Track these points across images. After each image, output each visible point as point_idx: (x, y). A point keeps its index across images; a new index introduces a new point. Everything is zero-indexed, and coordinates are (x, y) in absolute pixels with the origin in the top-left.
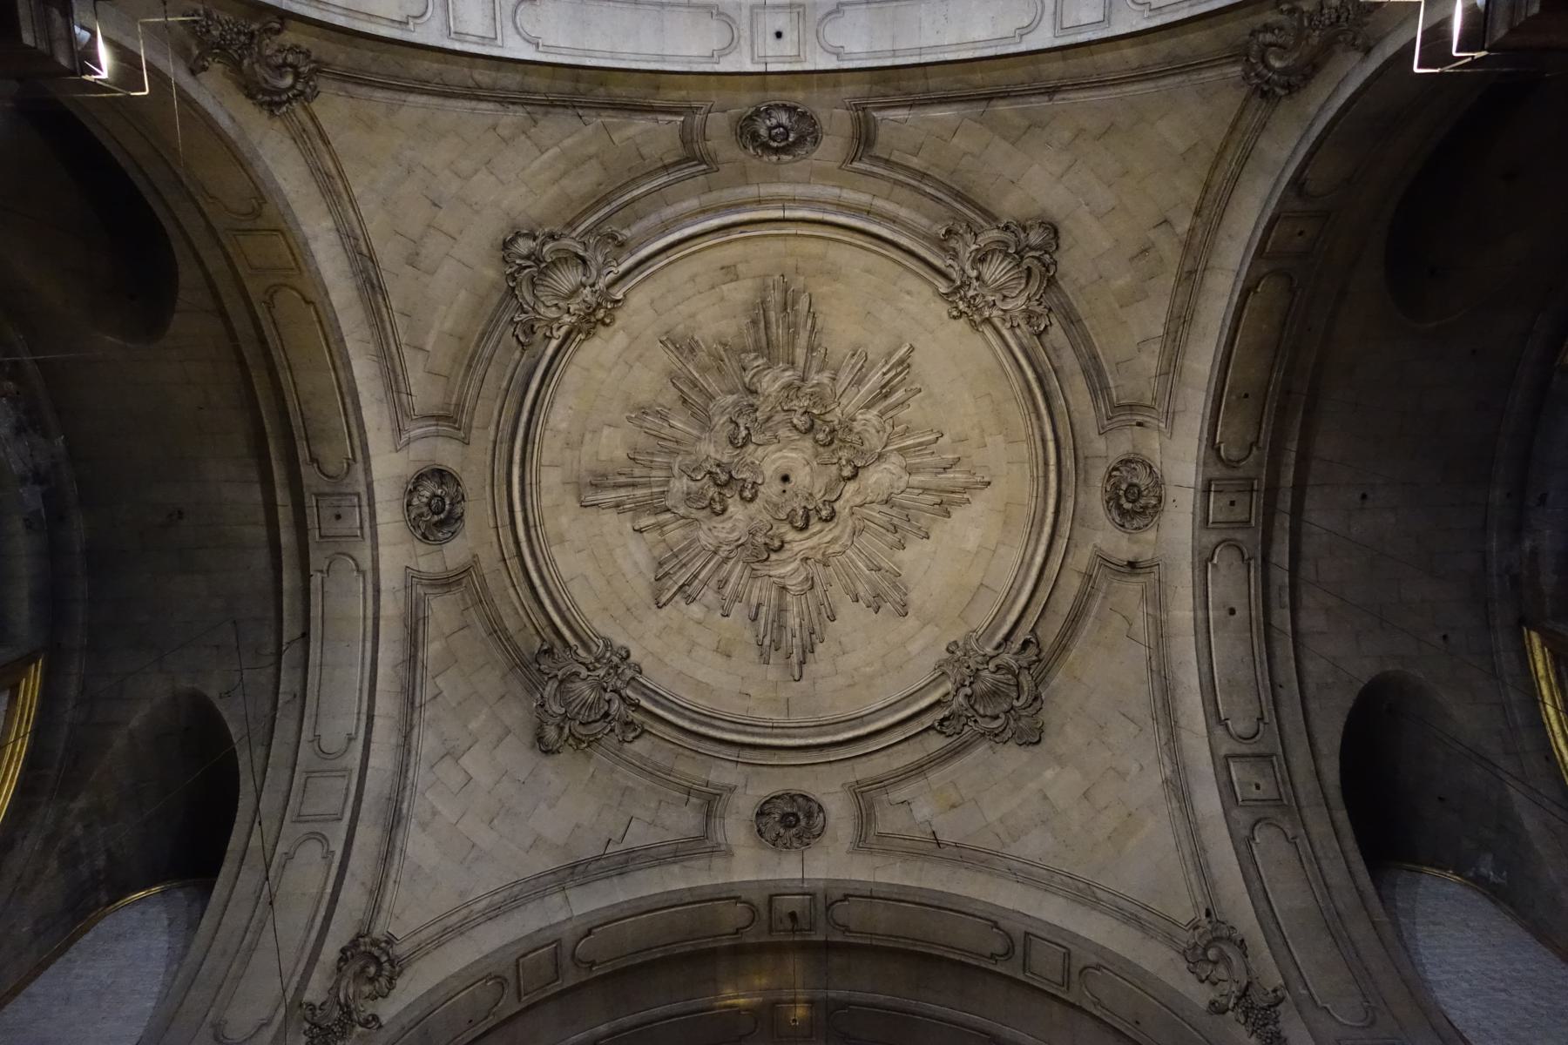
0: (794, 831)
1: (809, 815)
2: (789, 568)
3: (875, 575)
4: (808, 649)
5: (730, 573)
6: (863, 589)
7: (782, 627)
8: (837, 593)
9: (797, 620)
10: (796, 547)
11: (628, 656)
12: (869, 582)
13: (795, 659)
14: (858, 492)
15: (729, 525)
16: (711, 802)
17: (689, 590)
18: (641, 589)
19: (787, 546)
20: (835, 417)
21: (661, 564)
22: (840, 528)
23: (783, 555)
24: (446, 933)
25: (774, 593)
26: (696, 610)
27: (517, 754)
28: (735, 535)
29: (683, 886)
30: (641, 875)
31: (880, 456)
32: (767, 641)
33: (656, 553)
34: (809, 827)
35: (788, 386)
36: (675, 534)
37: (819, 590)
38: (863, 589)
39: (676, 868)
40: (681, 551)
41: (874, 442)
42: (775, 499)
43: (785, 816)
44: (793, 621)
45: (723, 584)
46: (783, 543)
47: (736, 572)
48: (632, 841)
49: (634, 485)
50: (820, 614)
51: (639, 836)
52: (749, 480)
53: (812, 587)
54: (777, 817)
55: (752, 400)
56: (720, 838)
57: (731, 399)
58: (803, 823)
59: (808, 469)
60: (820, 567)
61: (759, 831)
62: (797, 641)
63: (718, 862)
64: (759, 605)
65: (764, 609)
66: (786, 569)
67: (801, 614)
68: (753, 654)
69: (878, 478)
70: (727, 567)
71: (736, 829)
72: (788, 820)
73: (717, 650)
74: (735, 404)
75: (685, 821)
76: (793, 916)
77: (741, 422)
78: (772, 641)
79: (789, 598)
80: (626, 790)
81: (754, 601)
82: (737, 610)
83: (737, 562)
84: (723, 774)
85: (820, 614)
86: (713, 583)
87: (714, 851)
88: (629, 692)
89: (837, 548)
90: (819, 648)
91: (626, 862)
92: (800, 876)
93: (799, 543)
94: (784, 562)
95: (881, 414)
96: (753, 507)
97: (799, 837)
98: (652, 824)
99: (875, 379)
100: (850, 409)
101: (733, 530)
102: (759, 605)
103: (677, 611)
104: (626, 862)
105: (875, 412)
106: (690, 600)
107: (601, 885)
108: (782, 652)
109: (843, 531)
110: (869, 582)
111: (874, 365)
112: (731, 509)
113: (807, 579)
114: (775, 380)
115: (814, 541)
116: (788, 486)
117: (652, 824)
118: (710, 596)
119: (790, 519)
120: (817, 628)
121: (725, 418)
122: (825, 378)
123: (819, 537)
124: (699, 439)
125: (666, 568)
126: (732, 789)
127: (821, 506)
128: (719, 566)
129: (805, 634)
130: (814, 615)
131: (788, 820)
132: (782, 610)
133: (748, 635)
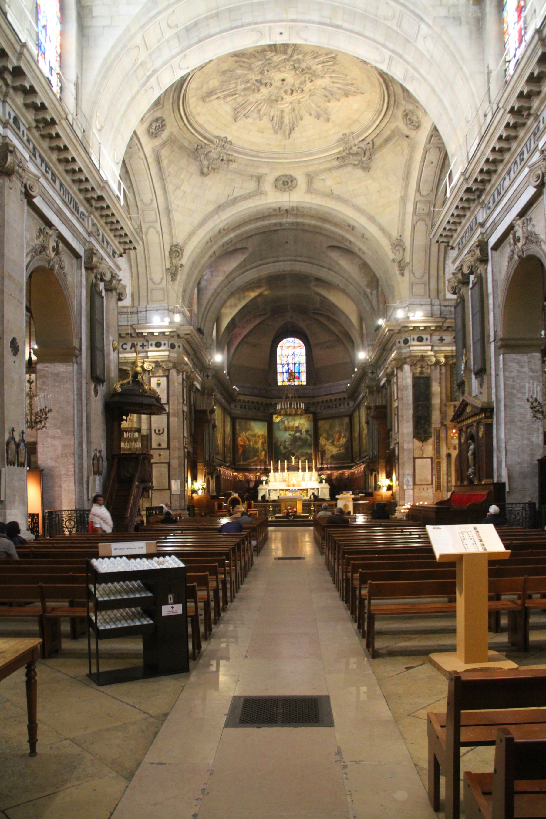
0: (287, 187)
1: (292, 181)
2: (285, 106)
3: (318, 109)
4: (292, 129)
5: (262, 107)
6: (313, 112)
7: (282, 123)
8: (303, 112)
9: (288, 121)
10: (287, 100)
11: (227, 139)
12: (315, 110)
13: (287, 132)
14: (312, 85)
15: (261, 95)
16: (259, 179)
17: (247, 115)
18: (230, 118)
19: (284, 100)
20: (303, 65)
21: (235, 109)
22: (305, 94)
23: (283, 102)
24: (191, 234)
25: (279, 113)
26: (250, 120)
27: (196, 179)
28: (263, 97)
29: (253, 205)
30: (240, 204)
31: (322, 77)
32: (277, 127)
33: (234, 106)
34: (291, 186)
35: (284, 59)
36: (240, 100)
37: (296, 112)
38: (313, 112)
39: (250, 200)
40: (243, 104)
41: (319, 72)
42: (279, 86)
43: (284, 182)
44: (286, 121)
45: (259, 111)
46: (282, 99)
47: (264, 108)
48: (235, 195)
49: (223, 91)
50: (296, 118)
51: (238, 193)
52: (269, 83)
53: (294, 110)
54: (281, 182)
55: (269, 62)
56: (263, 189)
57: (260, 63)
58: (290, 184)
59: (292, 78)
60: (297, 104)
61: (276, 186)
62: (288, 127)
63: (263, 197)
64: (273, 117)
65: (275, 118)
66: (285, 106)
67: (289, 119)
68: (272, 131)
69: (320, 82)
70: (260, 106)
71: (268, 186)
72: (285, 183)
73: (258, 131)
74: (262, 64)
75: (251, 186)
76: (286, 210)
77: (265, 69)
78: (279, 127)
79: (285, 114)
80: (231, 180)
81: (272, 115)
82: (266, 119)
83: (264, 104)
84: (263, 170)
85: (296, 118)
86: (256, 110)
87: (261, 193)
88: (229, 153)
89: (304, 99)
90: (296, 129)
91: (234, 201)
92: (288, 200)
93: (288, 98)
94: (283, 104)
95: (323, 67)
96: (271, 89)
97: (289, 188)
98: (241, 188)
99: (320, 59)
100: (311, 64)
101: (262, 96)
102: (273, 117)
103: (242, 122)
104: (234, 201)
105: (320, 66)
106: (247, 117)
107: (229, 209)
108: (282, 130)
109: (306, 95)
110: (315, 110)
111: (320, 55)
112: (261, 90)
113: (292, 109)
114: (278, 58)
115: (295, 98)
116: (284, 82)
117: (241, 188)
118: (255, 115)
119: (286, 92)
120: (295, 123)
121: (258, 68)
122: (300, 57)
123: (296, 96)
124: (248, 74)
125: (238, 110)
126: (266, 174)
127: (297, 89)
128: (258, 106)
129: (291, 125)
130: (295, 120)
131: (285, 183)
132: (282, 117)
133: (270, 125)
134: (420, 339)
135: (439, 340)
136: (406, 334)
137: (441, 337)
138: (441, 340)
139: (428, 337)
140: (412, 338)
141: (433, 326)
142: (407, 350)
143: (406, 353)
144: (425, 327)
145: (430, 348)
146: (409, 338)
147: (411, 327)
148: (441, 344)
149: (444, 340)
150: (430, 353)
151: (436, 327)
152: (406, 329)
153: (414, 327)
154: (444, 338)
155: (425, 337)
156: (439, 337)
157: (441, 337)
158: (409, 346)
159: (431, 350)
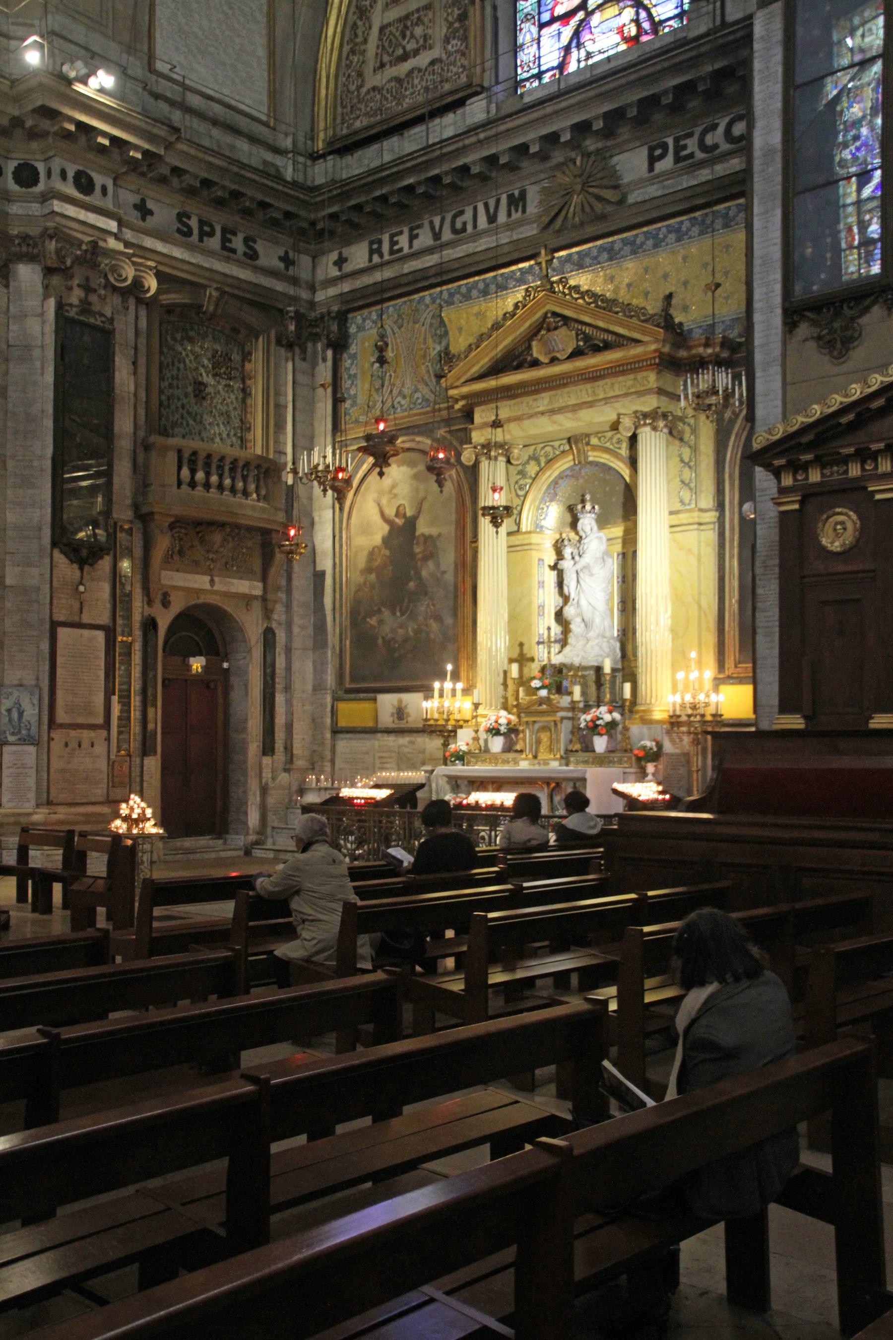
134: (84, 184)
135: (136, 206)
136: (35, 145)
137: (143, 201)
138: (143, 211)
139: (109, 183)
140: (56, 171)
141: (136, 148)
142: (36, 209)
143: (29, 219)
144: (114, 139)
145: (113, 226)
146: (41, 167)
147: (71, 120)
148: (141, 223)
149: (151, 213)
150: (112, 243)
151: (146, 153)
152: (45, 124)
153: (80, 125)
154: (150, 205)
155: (99, 179)
156: (135, 199)
157: (143, 201)
158: (45, 197)
159: (117, 237)
